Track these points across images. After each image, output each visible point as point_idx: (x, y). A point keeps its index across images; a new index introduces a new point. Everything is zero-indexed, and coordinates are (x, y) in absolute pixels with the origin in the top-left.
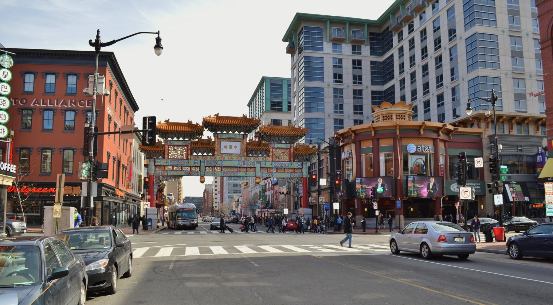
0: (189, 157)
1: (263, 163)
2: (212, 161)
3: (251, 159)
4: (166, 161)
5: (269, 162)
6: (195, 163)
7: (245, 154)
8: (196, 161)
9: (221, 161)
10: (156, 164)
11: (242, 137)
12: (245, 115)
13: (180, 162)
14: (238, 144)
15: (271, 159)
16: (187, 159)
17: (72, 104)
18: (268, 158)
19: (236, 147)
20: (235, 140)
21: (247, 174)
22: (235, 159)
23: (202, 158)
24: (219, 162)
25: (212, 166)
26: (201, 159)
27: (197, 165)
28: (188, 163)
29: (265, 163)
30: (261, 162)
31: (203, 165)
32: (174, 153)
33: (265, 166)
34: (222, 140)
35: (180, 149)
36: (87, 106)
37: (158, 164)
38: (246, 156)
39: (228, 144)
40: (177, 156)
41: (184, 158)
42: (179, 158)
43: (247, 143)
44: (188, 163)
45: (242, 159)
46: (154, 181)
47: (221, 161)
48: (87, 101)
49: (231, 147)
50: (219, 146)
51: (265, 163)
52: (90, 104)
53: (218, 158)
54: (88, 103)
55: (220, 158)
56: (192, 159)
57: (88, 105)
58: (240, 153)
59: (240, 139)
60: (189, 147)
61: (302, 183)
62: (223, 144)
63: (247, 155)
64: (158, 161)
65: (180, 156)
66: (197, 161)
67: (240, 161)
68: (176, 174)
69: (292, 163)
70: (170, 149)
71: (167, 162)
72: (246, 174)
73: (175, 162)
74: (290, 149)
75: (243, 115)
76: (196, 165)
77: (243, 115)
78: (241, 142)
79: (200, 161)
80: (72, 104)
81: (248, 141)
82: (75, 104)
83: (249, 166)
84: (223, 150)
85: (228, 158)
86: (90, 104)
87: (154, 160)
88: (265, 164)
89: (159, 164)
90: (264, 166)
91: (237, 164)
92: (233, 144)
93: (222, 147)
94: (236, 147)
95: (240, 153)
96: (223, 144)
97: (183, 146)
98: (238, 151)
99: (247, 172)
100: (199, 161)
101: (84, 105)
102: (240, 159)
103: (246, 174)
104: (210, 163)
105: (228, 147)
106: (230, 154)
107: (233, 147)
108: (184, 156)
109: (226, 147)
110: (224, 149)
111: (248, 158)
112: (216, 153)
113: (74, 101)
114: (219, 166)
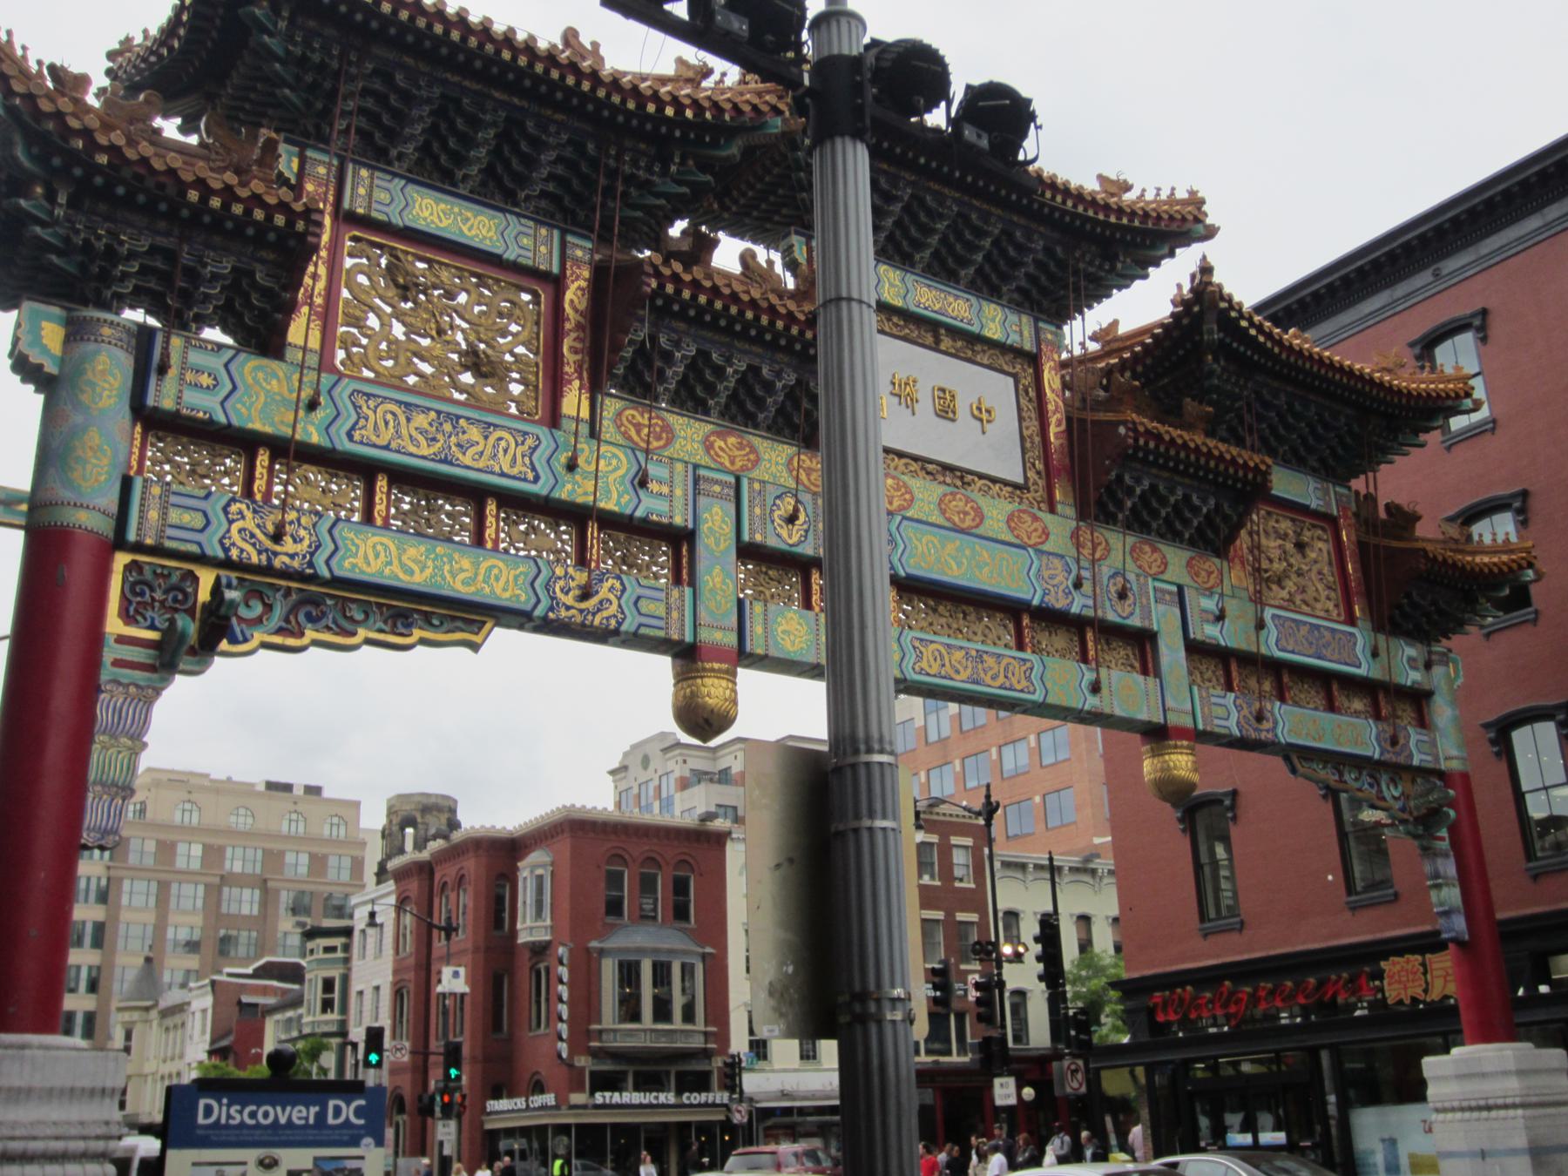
0: (574, 401)
4: (307, 393)
6: (642, 481)
8: (653, 470)
10: (163, 395)
13: (474, 433)
19: (982, 415)
20: (970, 344)
23: (708, 447)
28: (572, 466)
29: (1210, 604)
30: (1189, 595)
32: (398, 330)
35: (462, 298)
40: (426, 368)
46: (114, 624)
56: (608, 429)
60: (575, 295)
64: (195, 357)
65: (467, 378)
68: (418, 579)
70: (349, 262)
72: (1095, 688)
73: (421, 420)
76: (651, 507)
78: (1015, 376)
79: (696, 480)
85: (942, 506)
89: (203, 404)
90: (1210, 632)
97: (515, 267)
104: (791, 519)
106: (947, 468)
109: (904, 393)
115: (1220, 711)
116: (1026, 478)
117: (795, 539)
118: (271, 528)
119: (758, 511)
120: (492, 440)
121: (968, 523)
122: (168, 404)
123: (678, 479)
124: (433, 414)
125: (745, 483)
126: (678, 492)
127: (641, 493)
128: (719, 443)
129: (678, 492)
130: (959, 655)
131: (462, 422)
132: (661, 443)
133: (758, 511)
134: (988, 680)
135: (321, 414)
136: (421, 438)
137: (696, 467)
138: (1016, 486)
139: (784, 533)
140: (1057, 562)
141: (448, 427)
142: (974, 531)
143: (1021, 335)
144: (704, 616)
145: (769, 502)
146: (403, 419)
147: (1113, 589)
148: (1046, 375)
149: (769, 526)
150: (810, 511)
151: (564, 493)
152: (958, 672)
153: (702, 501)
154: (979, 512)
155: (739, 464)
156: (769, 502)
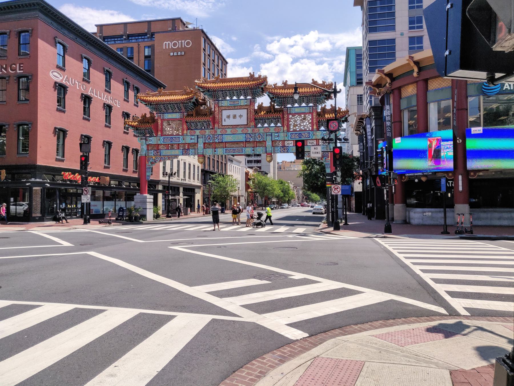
0: (185, 132)
1: (276, 134)
2: (211, 136)
3: (259, 130)
5: (283, 133)
6: (191, 139)
7: (253, 124)
9: (223, 135)
10: (147, 143)
11: (248, 103)
12: (252, 74)
13: (174, 138)
14: (244, 112)
15: (285, 128)
16: (183, 135)
17: (3, 70)
18: (282, 128)
19: (241, 116)
20: (240, 107)
21: (255, 150)
22: (239, 131)
23: (200, 132)
25: (211, 142)
27: (194, 141)
29: (277, 134)
31: (201, 141)
32: (169, 129)
33: (277, 138)
34: (223, 108)
36: (18, 71)
37: (150, 142)
38: (254, 127)
39: (232, 112)
40: (171, 132)
41: (180, 134)
42: (175, 134)
43: (255, 110)
44: (184, 139)
45: (248, 131)
46: (147, 163)
47: (223, 135)
48: (18, 65)
49: (235, 117)
50: (220, 117)
52: (21, 68)
53: (219, 132)
54: (20, 67)
55: (221, 132)
56: (188, 134)
57: (20, 70)
58: (246, 124)
59: (246, 105)
61: (329, 159)
62: (225, 113)
63: (256, 126)
65: (175, 132)
67: (245, 134)
69: (315, 132)
71: (159, 140)
74: (312, 114)
75: (250, 73)
77: (250, 73)
78: (247, 109)
80: (3, 70)
81: (256, 108)
82: (6, 69)
83: (257, 140)
84: (225, 121)
85: (231, 131)
86: (21, 68)
87: (146, 138)
88: (278, 136)
91: (242, 138)
92: (238, 112)
93: (224, 117)
94: (241, 116)
95: (246, 124)
96: (225, 113)
98: (243, 121)
99: (255, 148)
100: (196, 137)
101: (15, 70)
102: (246, 132)
103: (253, 150)
105: (231, 117)
107: (237, 116)
108: (180, 131)
109: (228, 117)
110: (226, 119)
111: (256, 130)
112: (216, 126)
113: (4, 66)
114: (219, 141)
115: (277, 150)
116: (247, 123)
122: (148, 144)
130: (232, 150)
135: (160, 141)
137: (198, 136)
138: (245, 125)
143: (247, 103)
144: (199, 152)
147: (258, 136)
148: (251, 107)
151: (183, 142)
153: (199, 139)
154: (237, 131)
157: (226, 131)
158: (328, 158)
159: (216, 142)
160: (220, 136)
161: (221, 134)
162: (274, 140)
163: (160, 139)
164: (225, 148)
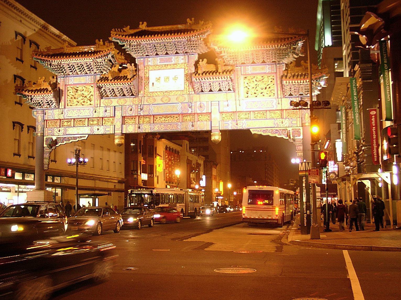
2: (134, 106)
8: (107, 109)
23: (118, 102)
24: (145, 109)
26: (116, 104)
31: (119, 114)
45: (185, 99)
51: (226, 103)
66: (109, 109)
73: (75, 111)
76: (107, 114)
79: (115, 108)
85: (161, 100)
87: (44, 111)
90: (227, 109)
94: (175, 78)
100: (112, 109)
104: (131, 110)
117: (131, 113)
118: (58, 130)
119: (125, 111)
120: (84, 111)
121: (167, 101)
123: (112, 109)
124: (77, 110)
125: (123, 106)
126: (112, 111)
127: (106, 113)
128: (119, 101)
129: (112, 111)
131: (80, 110)
132: (110, 104)
133: (125, 111)
134: (168, 129)
136: (75, 114)
137: (115, 106)
139: (129, 113)
140: (186, 104)
141: (79, 111)
142: (168, 103)
145: (127, 108)
146: (73, 112)
149: (127, 112)
150: (134, 108)
152: (162, 129)
153: (116, 111)
155: (123, 104)
156: (127, 108)
157: (155, 99)
158: (299, 136)
159: (139, 115)
160: (145, 106)
161: (148, 104)
162: (222, 111)
163: (63, 113)
164: (154, 123)
